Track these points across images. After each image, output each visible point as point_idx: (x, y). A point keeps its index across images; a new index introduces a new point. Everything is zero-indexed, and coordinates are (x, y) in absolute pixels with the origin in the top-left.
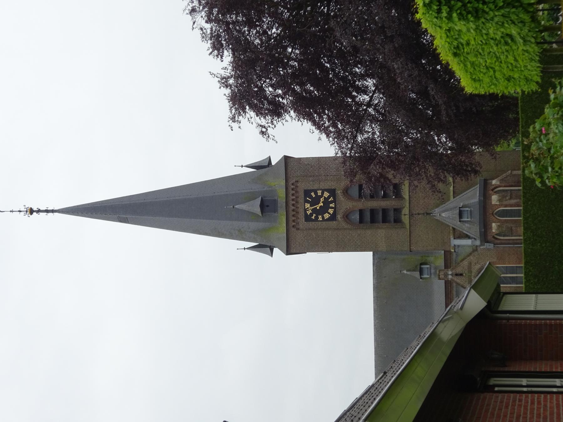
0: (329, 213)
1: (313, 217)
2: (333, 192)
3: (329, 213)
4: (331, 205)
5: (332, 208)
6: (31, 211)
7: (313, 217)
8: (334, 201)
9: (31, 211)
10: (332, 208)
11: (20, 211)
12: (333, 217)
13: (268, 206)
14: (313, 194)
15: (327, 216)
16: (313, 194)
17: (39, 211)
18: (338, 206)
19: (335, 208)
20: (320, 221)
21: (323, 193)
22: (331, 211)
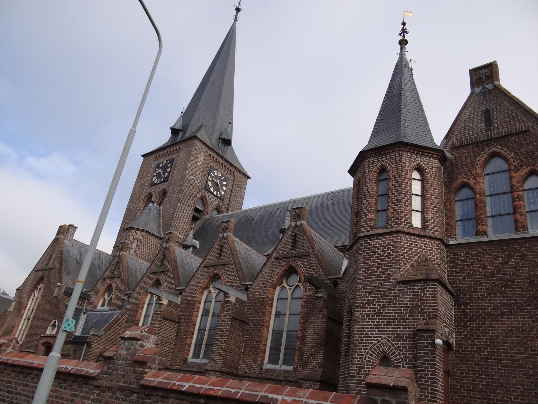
0: (211, 187)
1: (212, 173)
2: (221, 199)
3: (211, 187)
4: (215, 192)
5: (214, 191)
6: (238, 10)
7: (212, 173)
8: (216, 196)
9: (238, 10)
10: (214, 191)
11: (239, 4)
12: (207, 189)
13: (224, 146)
14: (225, 183)
15: (210, 184)
16: (225, 183)
17: (237, 13)
18: (213, 196)
19: (212, 193)
20: (208, 176)
21: (223, 190)
22: (212, 189)
